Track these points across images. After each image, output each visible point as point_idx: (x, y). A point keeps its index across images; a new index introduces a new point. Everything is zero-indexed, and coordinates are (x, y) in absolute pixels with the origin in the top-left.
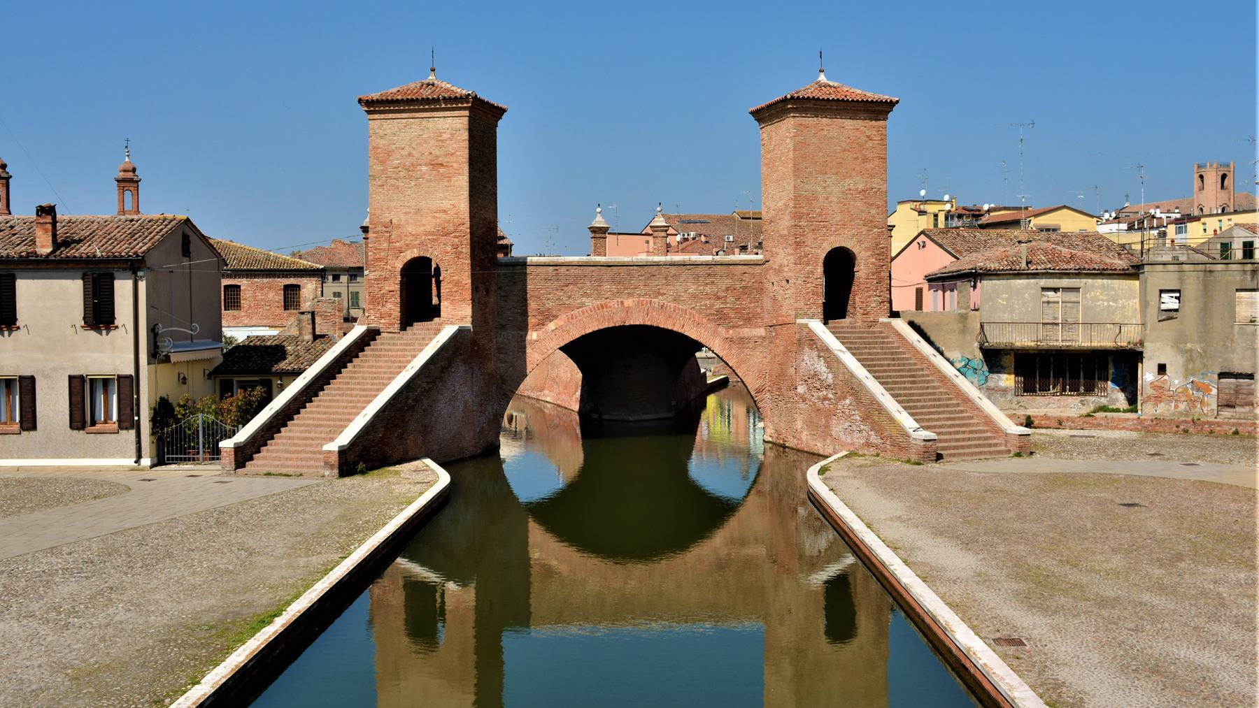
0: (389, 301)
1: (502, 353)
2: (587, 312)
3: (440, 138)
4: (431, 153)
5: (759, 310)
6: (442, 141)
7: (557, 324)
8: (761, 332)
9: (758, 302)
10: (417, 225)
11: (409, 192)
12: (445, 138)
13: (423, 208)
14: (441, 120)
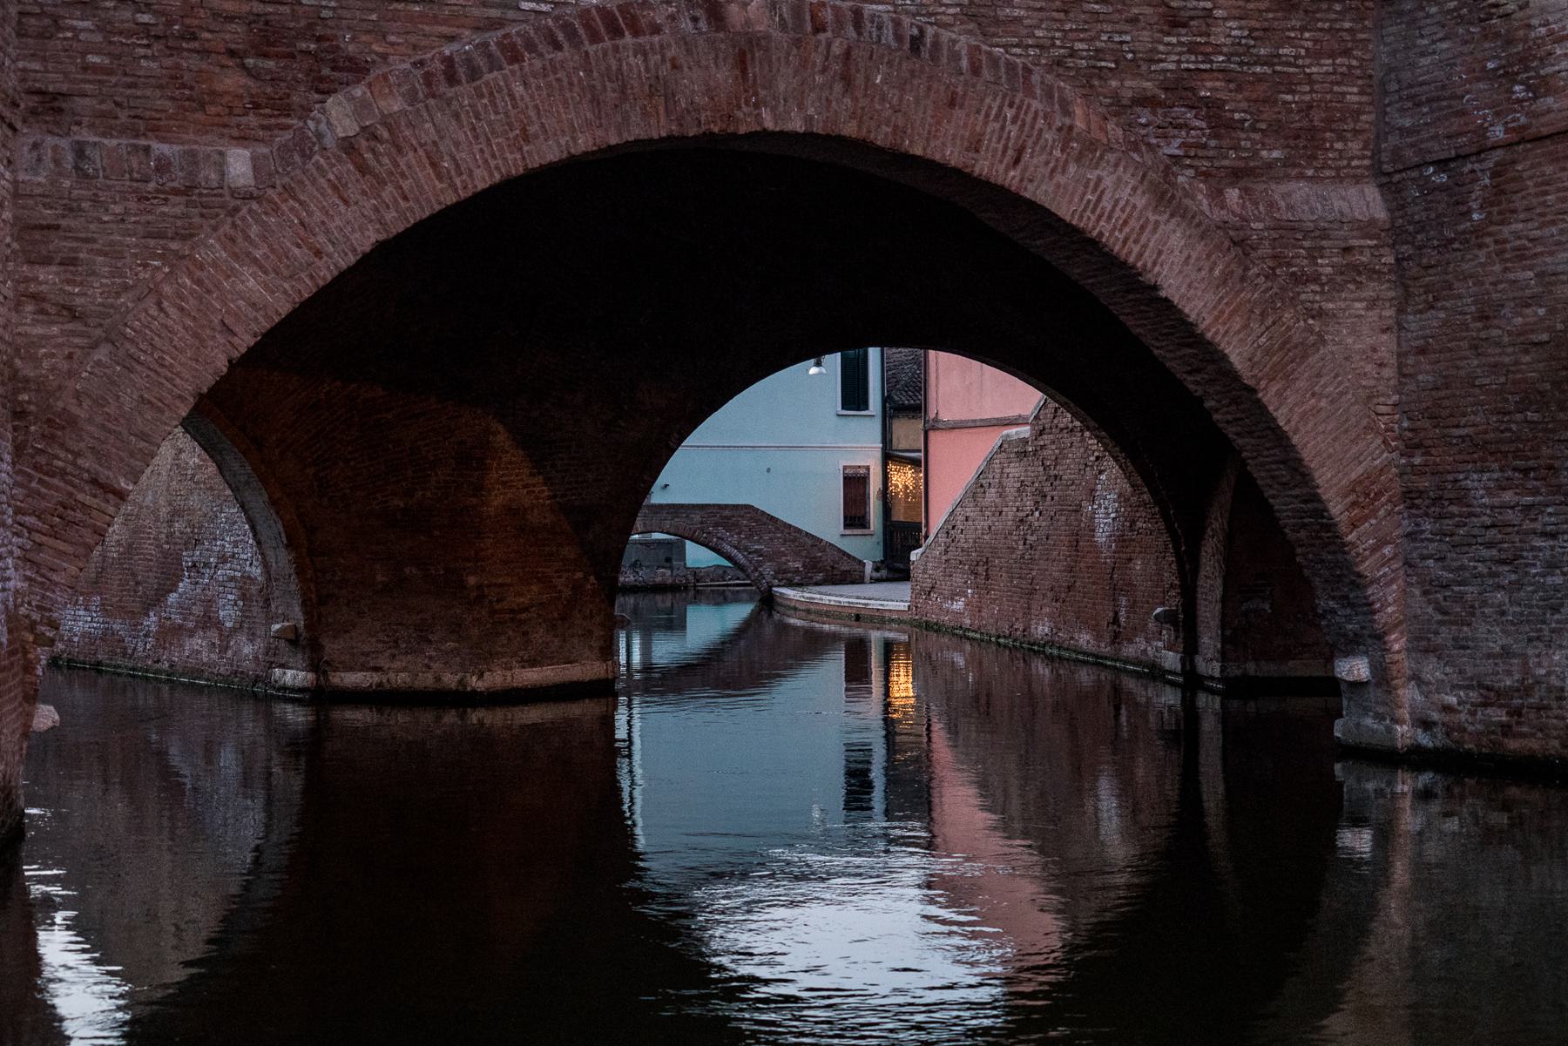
1: (46, 261)
2: (531, 46)
5: (1353, 95)
7: (362, 107)
8: (1367, 202)
9: (1346, 53)
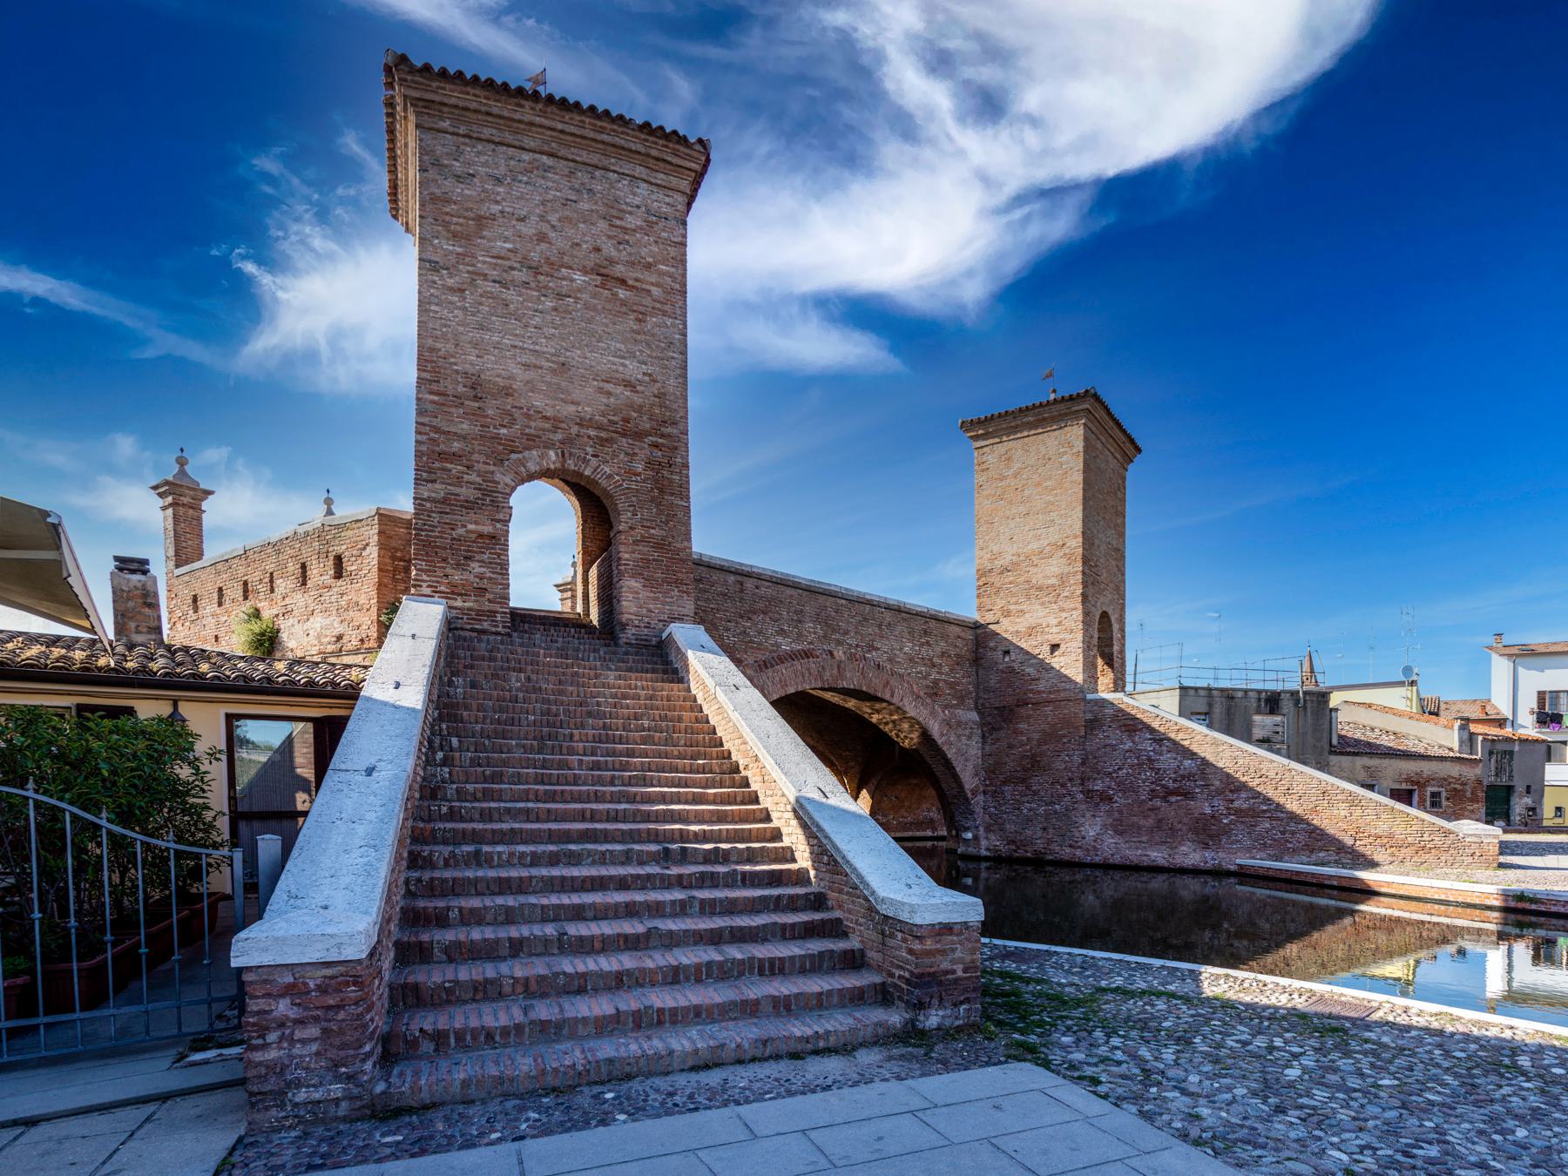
0: (477, 557)
3: (618, 223)
4: (598, 250)
6: (625, 230)
10: (556, 399)
11: (537, 320)
12: (633, 226)
13: (574, 363)
14: (625, 182)
